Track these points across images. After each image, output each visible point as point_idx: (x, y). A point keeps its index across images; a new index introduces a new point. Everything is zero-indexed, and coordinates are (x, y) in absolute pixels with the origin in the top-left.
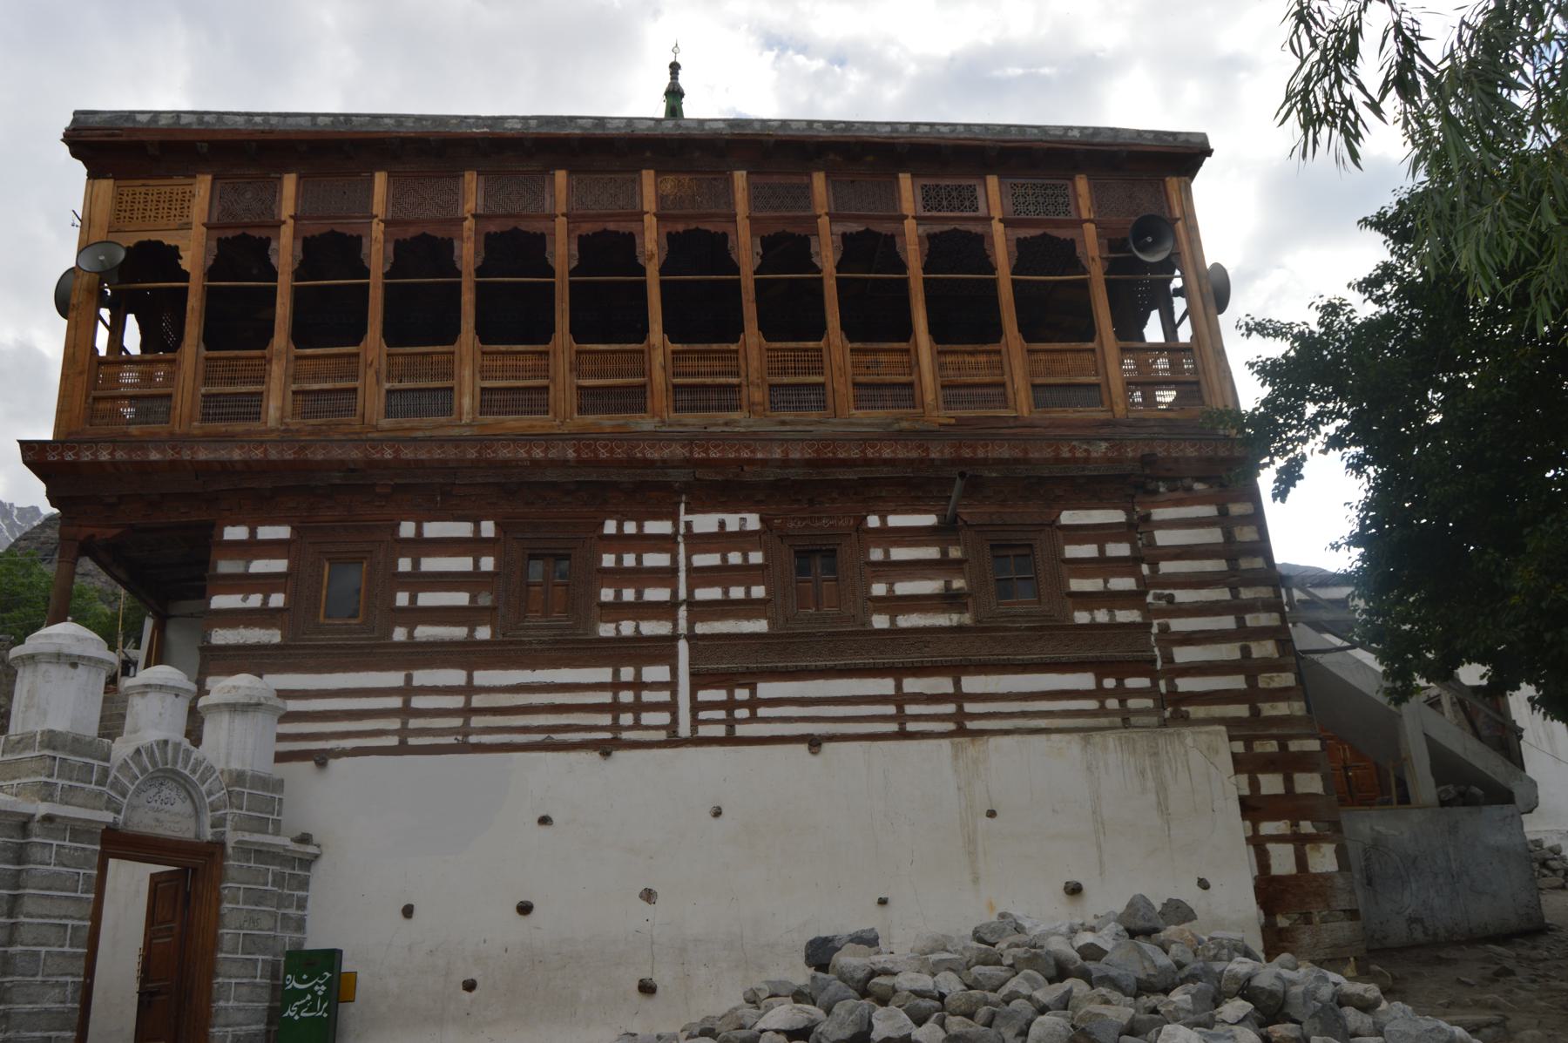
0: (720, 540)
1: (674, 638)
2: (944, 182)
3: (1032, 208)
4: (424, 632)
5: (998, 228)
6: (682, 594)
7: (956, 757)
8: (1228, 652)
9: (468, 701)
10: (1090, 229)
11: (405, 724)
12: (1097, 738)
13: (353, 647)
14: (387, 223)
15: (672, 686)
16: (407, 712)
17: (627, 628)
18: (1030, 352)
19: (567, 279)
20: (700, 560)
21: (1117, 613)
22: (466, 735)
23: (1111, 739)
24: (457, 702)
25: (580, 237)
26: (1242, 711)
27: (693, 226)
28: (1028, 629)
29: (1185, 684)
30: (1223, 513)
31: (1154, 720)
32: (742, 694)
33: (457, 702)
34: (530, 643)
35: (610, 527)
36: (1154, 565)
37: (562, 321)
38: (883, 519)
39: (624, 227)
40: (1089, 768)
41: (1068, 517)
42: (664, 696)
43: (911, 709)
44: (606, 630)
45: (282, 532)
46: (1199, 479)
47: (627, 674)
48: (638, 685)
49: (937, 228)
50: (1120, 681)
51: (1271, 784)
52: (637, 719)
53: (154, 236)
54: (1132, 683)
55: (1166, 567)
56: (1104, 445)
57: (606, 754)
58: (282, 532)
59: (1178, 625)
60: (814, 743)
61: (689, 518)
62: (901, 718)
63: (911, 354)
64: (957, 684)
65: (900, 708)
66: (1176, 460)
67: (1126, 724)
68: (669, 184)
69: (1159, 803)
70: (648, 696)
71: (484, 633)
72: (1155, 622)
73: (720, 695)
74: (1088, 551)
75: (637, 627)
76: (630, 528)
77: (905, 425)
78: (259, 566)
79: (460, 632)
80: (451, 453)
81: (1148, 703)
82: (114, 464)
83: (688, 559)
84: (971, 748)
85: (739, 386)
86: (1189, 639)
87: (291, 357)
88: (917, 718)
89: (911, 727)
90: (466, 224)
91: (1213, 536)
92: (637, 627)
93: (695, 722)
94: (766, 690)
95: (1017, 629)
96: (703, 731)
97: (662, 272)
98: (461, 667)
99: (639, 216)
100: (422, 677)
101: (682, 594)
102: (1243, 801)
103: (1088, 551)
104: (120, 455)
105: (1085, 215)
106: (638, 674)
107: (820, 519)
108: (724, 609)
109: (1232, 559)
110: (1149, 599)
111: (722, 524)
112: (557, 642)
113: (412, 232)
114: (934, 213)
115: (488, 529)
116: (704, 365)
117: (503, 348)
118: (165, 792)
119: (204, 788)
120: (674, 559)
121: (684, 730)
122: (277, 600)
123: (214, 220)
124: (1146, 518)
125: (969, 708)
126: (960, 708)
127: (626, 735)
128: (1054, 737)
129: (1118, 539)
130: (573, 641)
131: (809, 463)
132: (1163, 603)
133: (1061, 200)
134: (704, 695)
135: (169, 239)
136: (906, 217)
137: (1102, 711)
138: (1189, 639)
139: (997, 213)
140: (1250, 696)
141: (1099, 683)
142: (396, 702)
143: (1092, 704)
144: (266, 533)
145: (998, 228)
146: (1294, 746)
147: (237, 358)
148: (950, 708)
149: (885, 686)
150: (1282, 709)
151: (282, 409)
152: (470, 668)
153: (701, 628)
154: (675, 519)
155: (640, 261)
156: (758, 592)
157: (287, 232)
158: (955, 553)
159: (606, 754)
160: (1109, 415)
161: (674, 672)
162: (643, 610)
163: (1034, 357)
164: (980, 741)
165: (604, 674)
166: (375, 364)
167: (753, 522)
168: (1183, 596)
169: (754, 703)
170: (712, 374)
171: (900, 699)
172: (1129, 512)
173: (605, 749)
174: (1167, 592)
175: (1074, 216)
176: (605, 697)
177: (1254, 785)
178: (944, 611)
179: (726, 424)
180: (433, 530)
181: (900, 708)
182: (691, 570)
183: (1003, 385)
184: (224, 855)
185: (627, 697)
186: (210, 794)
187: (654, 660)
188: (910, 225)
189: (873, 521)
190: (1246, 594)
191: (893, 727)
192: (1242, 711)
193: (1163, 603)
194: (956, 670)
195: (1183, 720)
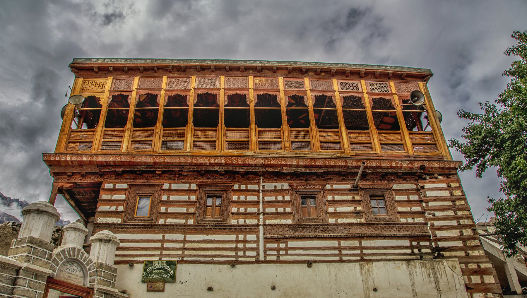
0: (275, 191)
1: (258, 225)
2: (347, 82)
3: (376, 90)
4: (170, 221)
5: (366, 96)
6: (261, 210)
7: (361, 269)
8: (455, 233)
9: (184, 245)
10: (396, 97)
11: (161, 252)
12: (412, 263)
13: (146, 225)
14: (166, 91)
15: (257, 242)
16: (162, 248)
17: (241, 221)
18: (379, 133)
19: (224, 108)
20: (267, 199)
21: (416, 219)
22: (183, 257)
23: (417, 263)
24: (180, 245)
25: (228, 95)
26: (462, 254)
27: (265, 93)
28: (384, 224)
29: (441, 244)
30: (449, 186)
31: (432, 257)
32: (282, 245)
33: (180, 245)
34: (207, 226)
35: (236, 187)
36: (427, 202)
37: (221, 121)
38: (332, 186)
39: (242, 93)
40: (410, 273)
41: (395, 187)
42: (254, 246)
43: (344, 252)
44: (234, 222)
45: (125, 186)
46: (439, 175)
47: (241, 237)
48: (245, 242)
49: (346, 95)
50: (418, 243)
51: (476, 279)
52: (244, 254)
53: (93, 95)
54: (422, 244)
55: (431, 204)
56: (407, 162)
57: (233, 266)
58: (125, 186)
59: (437, 223)
60: (309, 264)
61: (263, 184)
62: (340, 255)
63: (339, 133)
64: (360, 243)
65: (340, 251)
66: (432, 168)
67: (422, 258)
68: (258, 80)
69: (436, 286)
70: (248, 246)
71: (191, 222)
72: (429, 222)
73: (275, 245)
74: (404, 198)
75: (245, 221)
76: (243, 187)
77: (338, 155)
78: (115, 197)
79: (182, 221)
80: (182, 160)
81: (429, 251)
83: (263, 198)
84: (367, 267)
85: (281, 142)
86: (441, 229)
87: (132, 130)
88: (346, 255)
89: (344, 258)
90: (191, 91)
91: (447, 194)
92: (245, 221)
93: (266, 255)
94: (291, 244)
95: (381, 224)
96: (268, 258)
97: (255, 106)
98: (182, 233)
99: (248, 89)
100: (168, 236)
101: (261, 210)
102: (466, 286)
103: (404, 198)
104: (74, 159)
105: (394, 92)
106: (245, 237)
107: (310, 185)
108: (277, 215)
109: (453, 201)
110: (426, 214)
111: (275, 187)
112: (216, 226)
113: (174, 93)
114: (344, 90)
115: (194, 186)
116: (269, 135)
117: (201, 128)
118: (73, 267)
119: (87, 267)
120: (259, 198)
121: (261, 258)
122: (121, 208)
123: (112, 89)
124: (423, 187)
125: (365, 252)
126: (362, 251)
127: (240, 259)
128: (396, 262)
129: (413, 194)
130: (222, 226)
131: (305, 166)
132: (431, 216)
133: (385, 88)
134: (268, 246)
135: (97, 95)
136: (336, 91)
137: (413, 253)
138: (441, 229)
139: (365, 91)
140: (465, 248)
141: (411, 244)
142: (159, 245)
143: (409, 251)
144: (118, 186)
145: (366, 96)
146: (483, 266)
147: (115, 131)
148: (358, 252)
149: (335, 243)
150: (476, 253)
151: (128, 146)
152: (185, 234)
153: (267, 222)
154: (258, 184)
155: (248, 103)
156: (288, 210)
157: (134, 93)
158: (357, 198)
159: (233, 266)
160: (407, 154)
161: (258, 237)
162: (246, 215)
163: (380, 135)
164: (370, 265)
165: (233, 237)
166: (159, 132)
167: (286, 186)
168: (438, 214)
169: (286, 249)
170: (272, 138)
171: (340, 249)
172: (417, 185)
173: (233, 264)
174: (432, 212)
175: (390, 92)
176: (233, 246)
177: (470, 279)
178: (355, 218)
179: (277, 154)
180: (174, 186)
181: (340, 251)
182: (264, 202)
183: (371, 143)
184: (93, 293)
185: (241, 245)
186: (90, 270)
187: (251, 232)
188: (337, 94)
189: (328, 187)
190: (460, 213)
191: (338, 258)
192: (462, 254)
193: (431, 216)
194: (360, 238)
195: (443, 257)
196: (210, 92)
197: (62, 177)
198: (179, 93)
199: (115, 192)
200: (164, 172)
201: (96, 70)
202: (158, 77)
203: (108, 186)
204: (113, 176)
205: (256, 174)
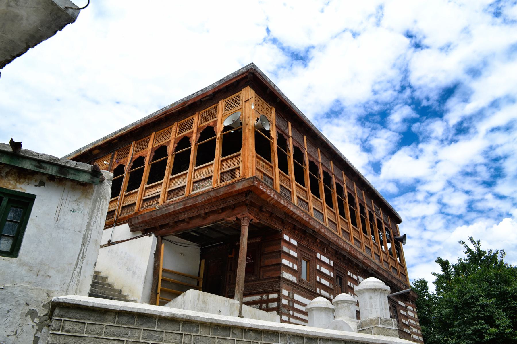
82: (273, 199)
180: (324, 259)
196: (329, 173)
197: (255, 209)
198: (314, 161)
199: (290, 246)
200: (321, 242)
201: (268, 92)
202: (300, 133)
203: (286, 237)
204: (290, 228)
205: (357, 266)
